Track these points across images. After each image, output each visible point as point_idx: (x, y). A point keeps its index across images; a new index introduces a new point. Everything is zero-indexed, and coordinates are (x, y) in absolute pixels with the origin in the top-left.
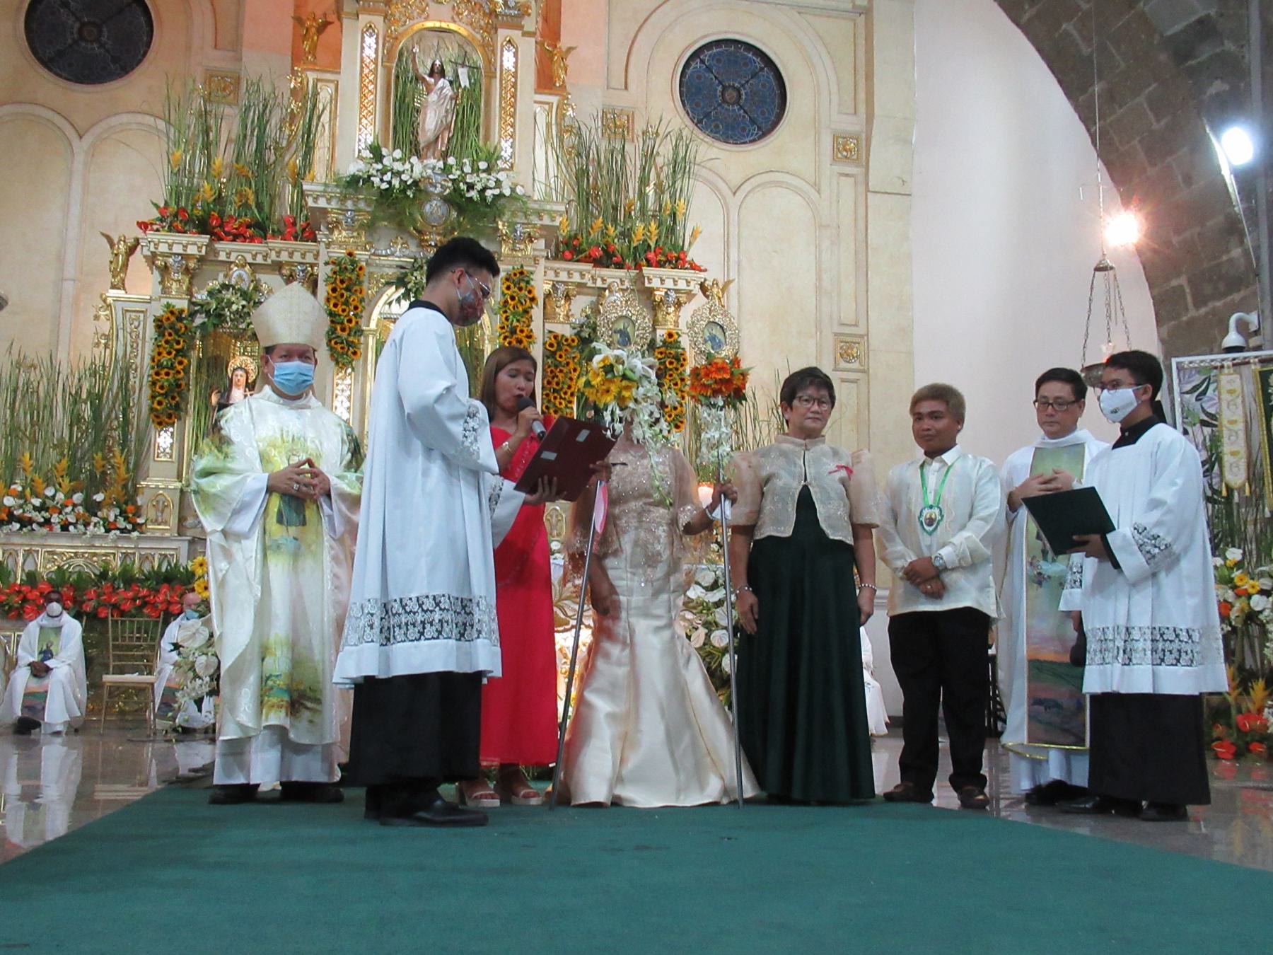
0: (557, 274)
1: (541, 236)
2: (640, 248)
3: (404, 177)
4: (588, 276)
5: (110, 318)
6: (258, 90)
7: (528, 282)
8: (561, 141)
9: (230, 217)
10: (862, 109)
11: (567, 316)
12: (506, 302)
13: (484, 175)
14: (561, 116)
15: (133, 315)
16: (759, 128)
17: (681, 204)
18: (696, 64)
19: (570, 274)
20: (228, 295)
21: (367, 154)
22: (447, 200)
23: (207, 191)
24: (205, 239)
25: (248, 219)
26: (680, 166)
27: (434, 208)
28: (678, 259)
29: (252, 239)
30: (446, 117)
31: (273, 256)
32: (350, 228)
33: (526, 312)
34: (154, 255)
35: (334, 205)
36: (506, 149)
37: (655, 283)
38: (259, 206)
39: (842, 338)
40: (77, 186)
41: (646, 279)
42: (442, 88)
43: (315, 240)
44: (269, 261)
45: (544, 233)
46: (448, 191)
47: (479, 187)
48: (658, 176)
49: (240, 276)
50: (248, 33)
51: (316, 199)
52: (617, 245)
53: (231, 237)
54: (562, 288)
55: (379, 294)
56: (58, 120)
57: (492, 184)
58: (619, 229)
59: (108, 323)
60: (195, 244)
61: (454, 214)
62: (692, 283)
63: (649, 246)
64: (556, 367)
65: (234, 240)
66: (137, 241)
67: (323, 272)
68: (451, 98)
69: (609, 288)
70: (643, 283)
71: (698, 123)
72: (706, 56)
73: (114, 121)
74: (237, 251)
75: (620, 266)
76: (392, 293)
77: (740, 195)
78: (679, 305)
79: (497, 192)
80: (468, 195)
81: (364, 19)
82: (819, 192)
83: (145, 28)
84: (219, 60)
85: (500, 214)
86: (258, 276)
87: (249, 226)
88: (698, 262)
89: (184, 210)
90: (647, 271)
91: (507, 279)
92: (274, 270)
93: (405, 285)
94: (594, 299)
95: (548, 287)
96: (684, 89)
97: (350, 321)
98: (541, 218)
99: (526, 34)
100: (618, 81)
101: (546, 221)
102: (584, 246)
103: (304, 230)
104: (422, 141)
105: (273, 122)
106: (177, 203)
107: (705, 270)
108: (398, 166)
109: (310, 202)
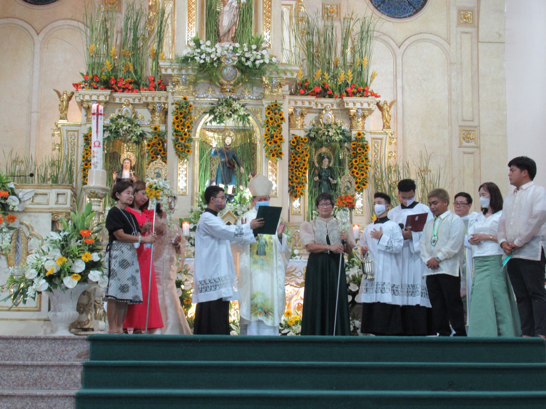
0: (296, 103)
1: (286, 83)
2: (342, 85)
3: (212, 56)
4: (313, 103)
5: (60, 135)
6: (133, 9)
7: (279, 110)
8: (297, 24)
9: (121, 78)
11: (302, 125)
12: (268, 121)
13: (254, 52)
15: (72, 133)
16: (414, 8)
17: (366, 59)
19: (303, 102)
20: (121, 121)
21: (192, 44)
22: (234, 67)
23: (108, 65)
24: (108, 92)
25: (130, 79)
27: (228, 71)
28: (364, 90)
29: (132, 90)
30: (234, 18)
31: (144, 100)
32: (184, 84)
33: (279, 126)
34: (82, 102)
35: (176, 72)
36: (266, 35)
37: (351, 105)
38: (136, 72)
40: (37, 60)
41: (345, 103)
43: (165, 90)
44: (142, 102)
45: (288, 81)
46: (235, 62)
47: (252, 59)
48: (353, 42)
49: (127, 111)
51: (166, 70)
52: (330, 84)
53: (121, 90)
54: (299, 110)
55: (200, 118)
56: (26, 25)
57: (259, 57)
58: (331, 74)
59: (59, 137)
60: (103, 95)
61: (239, 74)
62: (371, 105)
63: (348, 84)
64: (296, 154)
65: (123, 92)
66: (73, 93)
67: (171, 108)
68: (237, 8)
69: (325, 109)
70: (344, 106)
73: (55, 24)
74: (125, 97)
75: (331, 96)
76: (207, 118)
77: (403, 47)
78: (364, 117)
79: (262, 61)
80: (246, 64)
82: (449, 44)
85: (264, 74)
86: (136, 110)
87: (131, 83)
88: (375, 92)
89: (97, 76)
90: (346, 99)
91: (268, 109)
92: (144, 106)
93: (214, 113)
94: (317, 115)
95: (291, 110)
97: (185, 134)
98: (286, 74)
101: (289, 76)
102: (312, 86)
103: (159, 84)
104: (221, 33)
106: (92, 73)
107: (379, 96)
108: (209, 50)
109: (163, 72)
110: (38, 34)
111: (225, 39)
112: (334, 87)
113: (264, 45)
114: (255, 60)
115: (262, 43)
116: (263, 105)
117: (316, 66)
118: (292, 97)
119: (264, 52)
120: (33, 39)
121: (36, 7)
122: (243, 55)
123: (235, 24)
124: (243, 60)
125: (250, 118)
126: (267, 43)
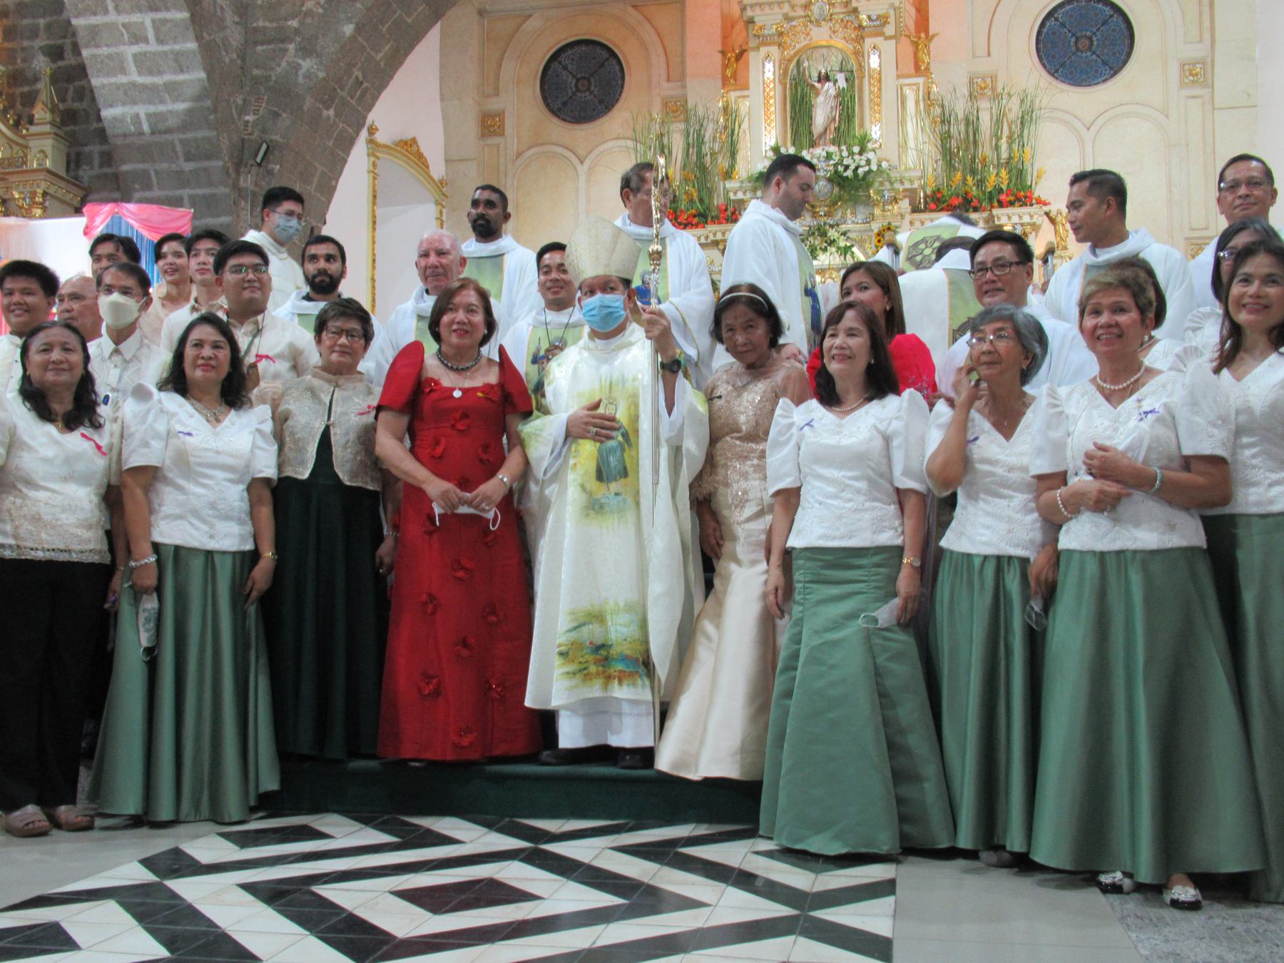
1: (905, 197)
2: (993, 192)
9: (682, 211)
10: (1207, 36)
13: (856, 157)
14: (928, 94)
16: (1111, 68)
17: (1027, 149)
18: (1052, 22)
22: (830, 180)
25: (694, 211)
26: (1026, 119)
29: (697, 226)
30: (832, 112)
31: (711, 237)
36: (875, 132)
37: (1004, 220)
38: (701, 201)
39: (1194, 241)
41: (996, 218)
42: (828, 90)
44: (709, 241)
45: (908, 194)
47: (852, 167)
50: (689, 69)
51: (735, 193)
52: (974, 191)
53: (683, 226)
57: (863, 163)
61: (836, 190)
62: (1035, 217)
63: (1002, 189)
68: (835, 97)
70: (994, 222)
71: (1053, 73)
72: (1059, 15)
79: (866, 169)
80: (845, 175)
81: (763, 50)
82: (1167, 116)
83: (620, 75)
84: (669, 90)
85: (869, 186)
88: (1043, 198)
90: (996, 212)
96: (1041, 46)
98: (902, 183)
99: (887, 38)
100: (982, 50)
101: (907, 185)
105: (706, 139)
107: (1049, 204)
110: (582, 163)
111: (821, 142)
112: (981, 195)
113: (870, 146)
114: (857, 168)
115: (869, 141)
116: (872, 231)
117: (954, 166)
118: (916, 216)
119: (871, 155)
120: (576, 169)
121: (577, 127)
122: (840, 162)
123: (834, 119)
124: (840, 169)
125: (855, 249)
126: (876, 142)
